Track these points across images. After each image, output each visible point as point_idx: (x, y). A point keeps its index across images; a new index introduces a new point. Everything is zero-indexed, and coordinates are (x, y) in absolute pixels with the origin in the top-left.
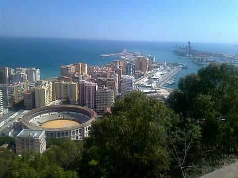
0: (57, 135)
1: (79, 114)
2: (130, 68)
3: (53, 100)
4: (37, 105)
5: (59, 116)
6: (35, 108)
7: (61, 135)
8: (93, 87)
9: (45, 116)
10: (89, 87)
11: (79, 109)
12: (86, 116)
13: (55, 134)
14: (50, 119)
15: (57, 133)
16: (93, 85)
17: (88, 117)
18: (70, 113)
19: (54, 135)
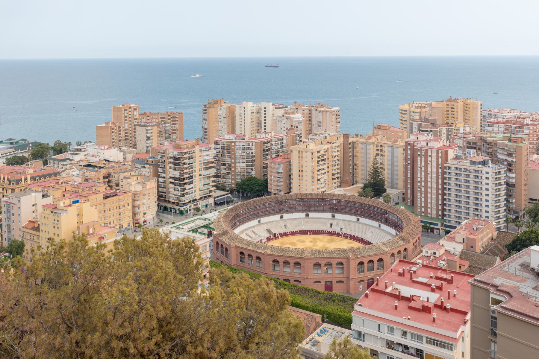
4: (295, 190)
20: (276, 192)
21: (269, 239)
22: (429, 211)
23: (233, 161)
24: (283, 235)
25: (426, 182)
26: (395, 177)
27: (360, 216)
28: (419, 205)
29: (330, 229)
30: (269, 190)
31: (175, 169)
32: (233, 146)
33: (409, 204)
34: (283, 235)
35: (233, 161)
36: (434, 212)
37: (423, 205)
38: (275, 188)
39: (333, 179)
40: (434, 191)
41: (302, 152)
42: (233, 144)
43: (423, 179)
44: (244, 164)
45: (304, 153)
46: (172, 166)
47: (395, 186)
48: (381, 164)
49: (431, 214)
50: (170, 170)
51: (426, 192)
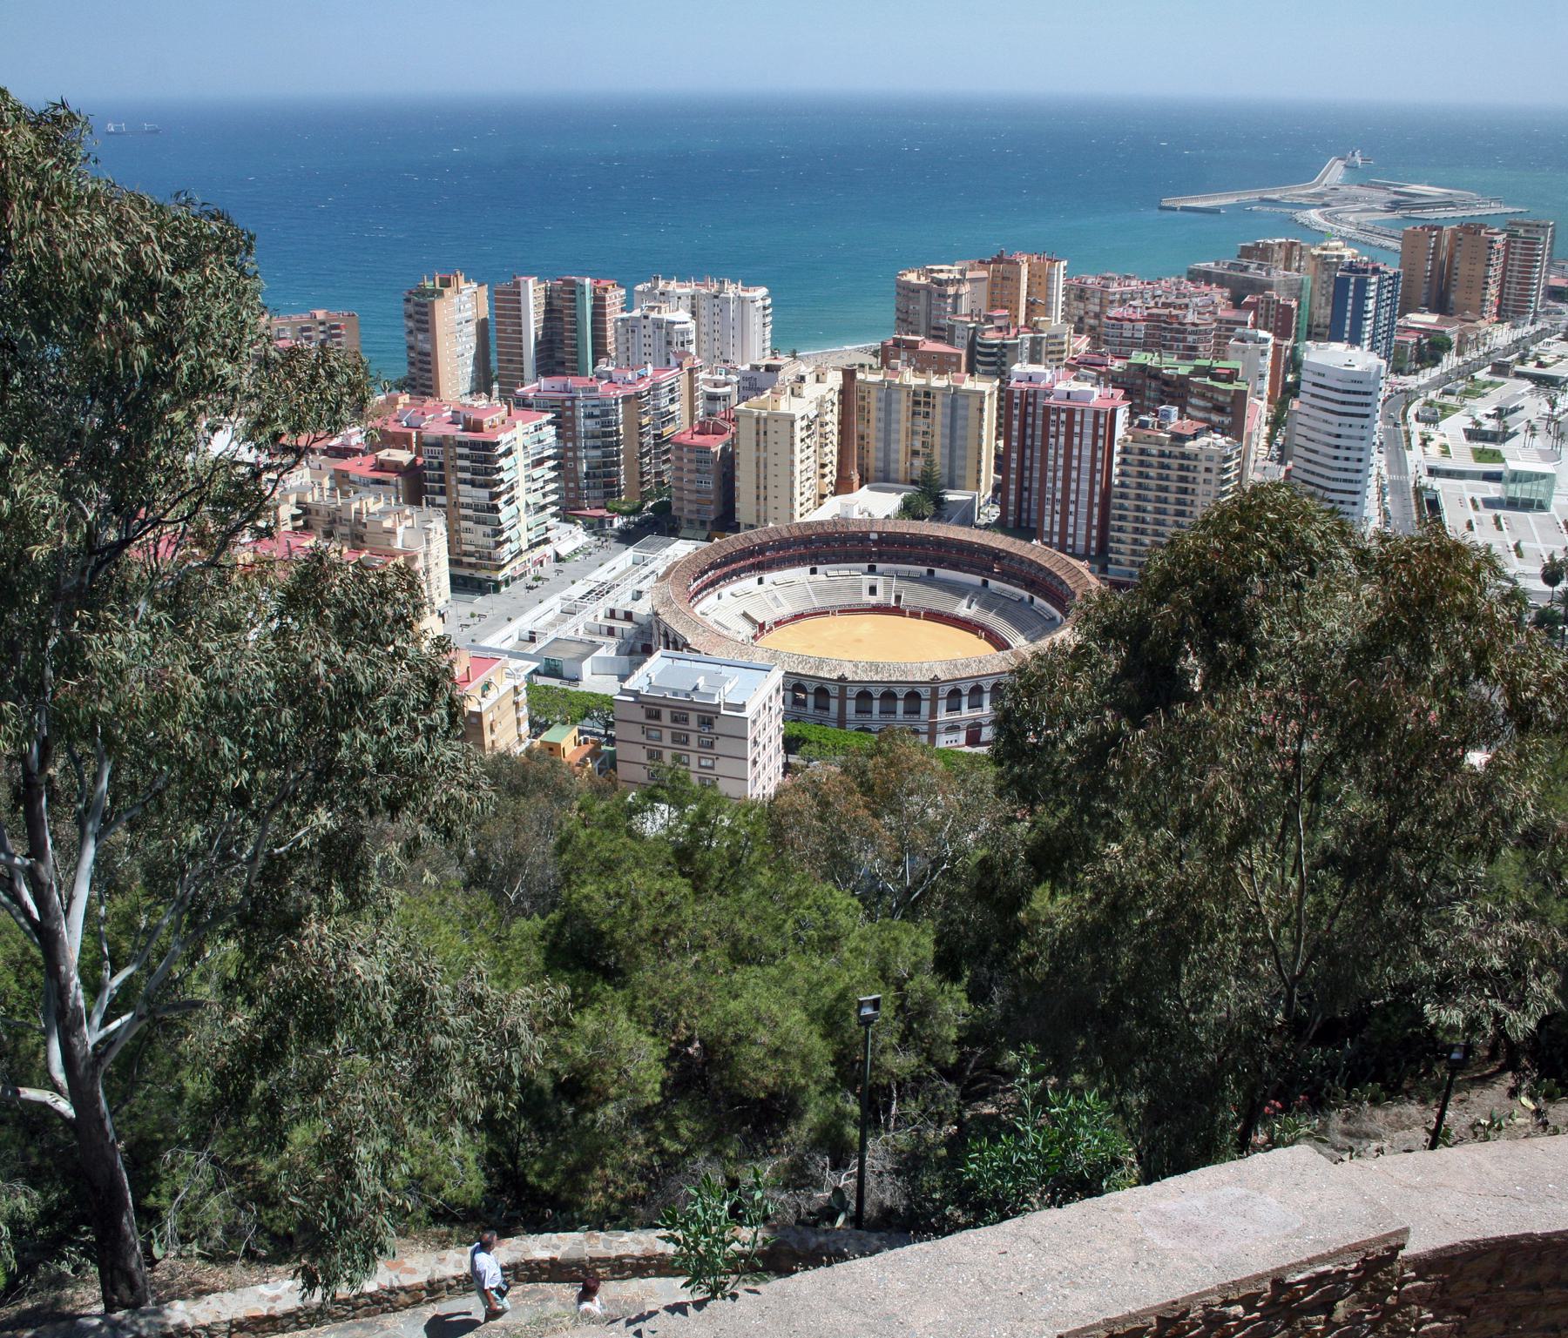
0: (851, 706)
1: (993, 584)
2: (1361, 298)
3: (843, 486)
4: (745, 508)
5: (873, 590)
6: (736, 528)
7: (876, 705)
8: (1097, 414)
9: (790, 583)
10: (1071, 413)
11: (997, 555)
12: (1037, 600)
13: (842, 699)
14: (817, 603)
15: (853, 692)
16: (1095, 401)
17: (1058, 615)
18: (940, 573)
19: (834, 704)
20: (694, 517)
21: (755, 637)
22: (1070, 541)
23: (570, 445)
24: (778, 623)
25: (1067, 480)
26: (958, 463)
27: (940, 563)
28: (1047, 529)
29: (873, 600)
30: (674, 512)
31: (473, 483)
32: (569, 408)
33: (1011, 526)
34: (778, 623)
35: (570, 445)
36: (1081, 543)
37: (1056, 529)
38: (694, 507)
39: (823, 476)
40: (1084, 499)
41: (766, 420)
42: (568, 403)
43: (1060, 474)
44: (598, 453)
45: (771, 423)
46: (467, 476)
47: (958, 482)
48: (925, 433)
49: (1073, 546)
50: (461, 487)
51: (1065, 501)
